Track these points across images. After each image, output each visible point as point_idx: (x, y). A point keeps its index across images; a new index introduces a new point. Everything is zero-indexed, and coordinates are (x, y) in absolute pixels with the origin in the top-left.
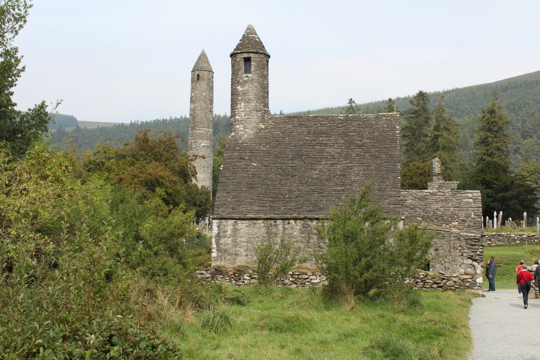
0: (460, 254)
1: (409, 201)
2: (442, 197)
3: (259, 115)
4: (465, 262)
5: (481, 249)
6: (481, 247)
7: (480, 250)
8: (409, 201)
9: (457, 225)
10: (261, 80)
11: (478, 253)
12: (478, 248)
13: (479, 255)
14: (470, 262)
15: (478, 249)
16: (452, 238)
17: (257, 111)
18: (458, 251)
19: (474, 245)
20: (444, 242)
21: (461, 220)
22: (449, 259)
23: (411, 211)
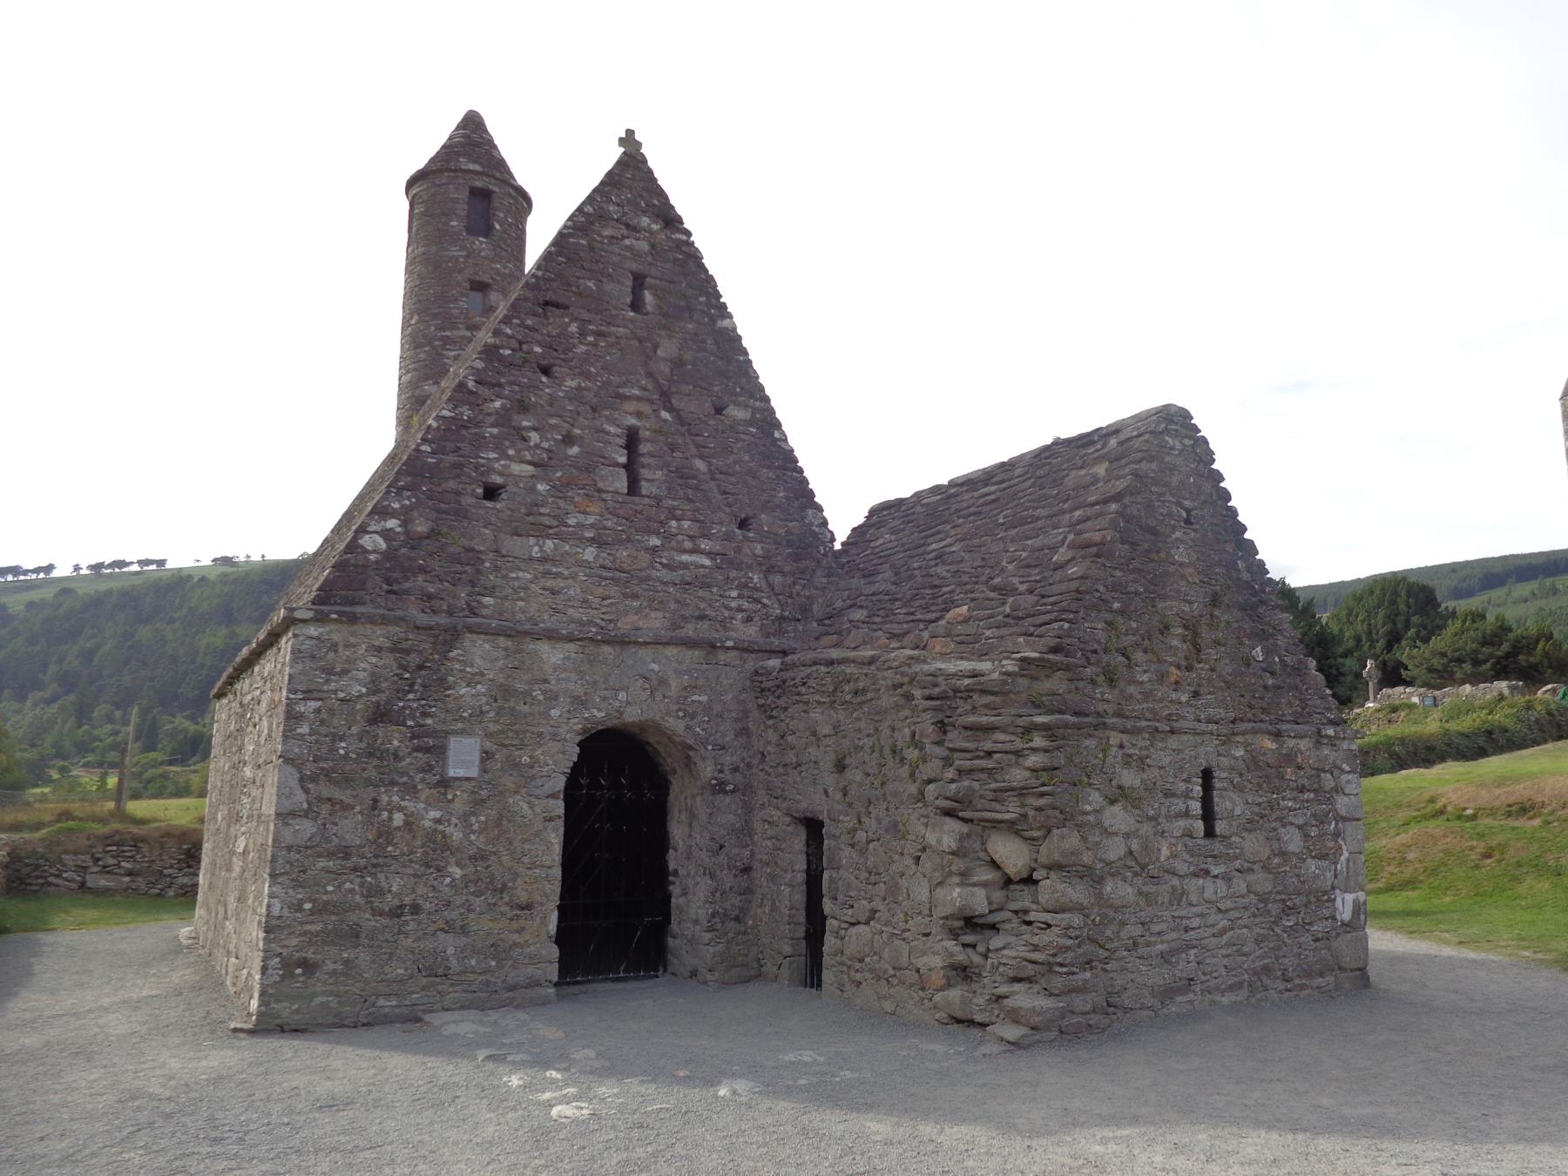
0: (913, 789)
1: (880, 541)
2: (993, 488)
3: (422, 356)
4: (931, 838)
5: (1034, 750)
6: (1038, 741)
7: (1033, 760)
8: (880, 541)
9: (966, 621)
10: (434, 249)
11: (1018, 776)
12: (1019, 744)
13: (1022, 792)
14: (946, 835)
15: (1018, 753)
16: (887, 700)
17: (416, 348)
18: (904, 771)
19: (992, 729)
20: (862, 724)
21: (994, 589)
22: (879, 821)
23: (862, 582)
